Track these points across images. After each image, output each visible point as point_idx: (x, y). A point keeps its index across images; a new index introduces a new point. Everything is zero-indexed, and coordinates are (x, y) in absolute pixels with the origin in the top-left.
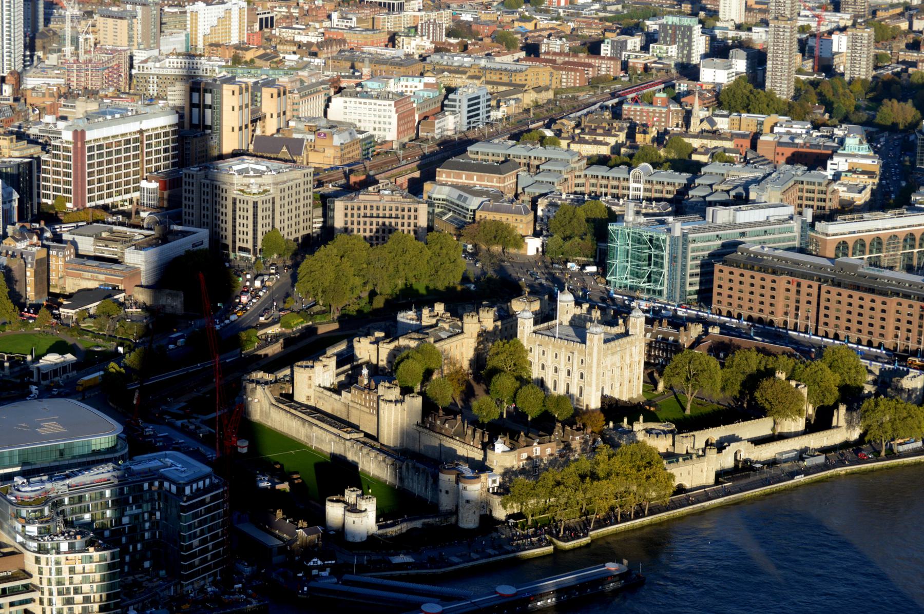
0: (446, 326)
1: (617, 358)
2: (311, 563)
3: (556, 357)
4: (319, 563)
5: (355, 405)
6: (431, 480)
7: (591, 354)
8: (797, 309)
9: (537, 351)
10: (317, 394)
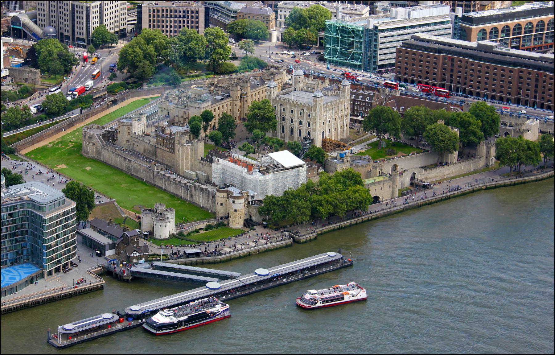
0: (220, 93)
2: (132, 255)
3: (292, 112)
4: (137, 254)
5: (160, 147)
6: (211, 197)
7: (315, 111)
8: (452, 76)
9: (279, 108)
10: (134, 139)
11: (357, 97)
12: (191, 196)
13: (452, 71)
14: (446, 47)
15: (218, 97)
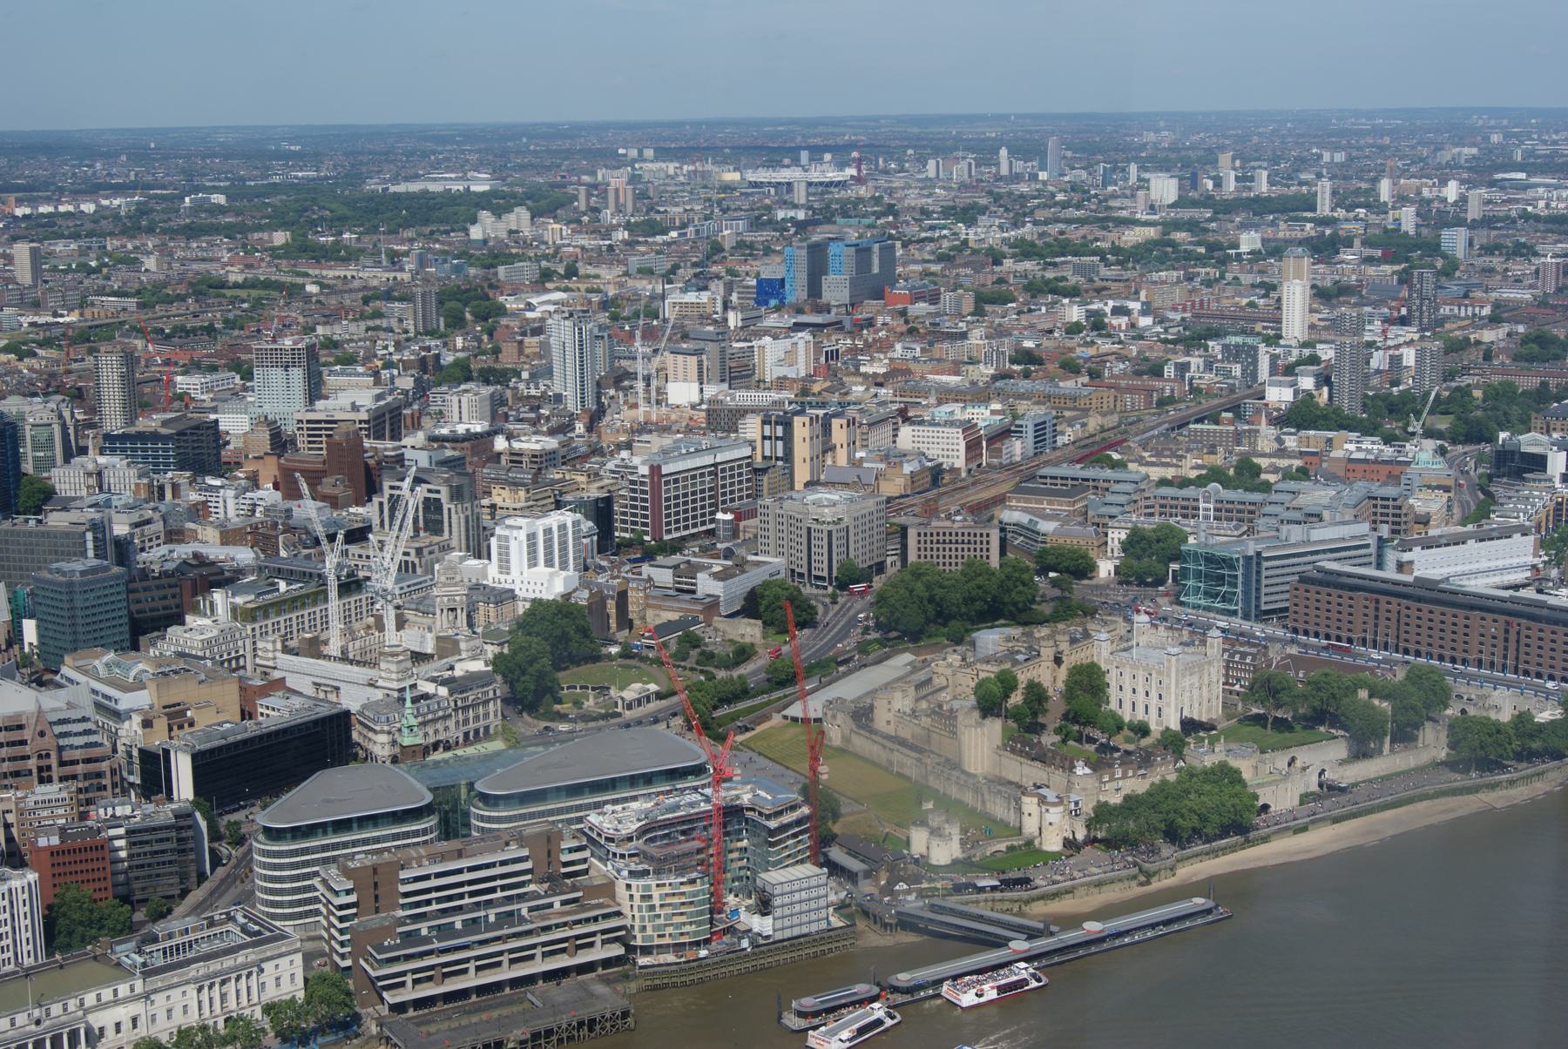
1: (1195, 679)
7: (1169, 676)
8: (1376, 625)
11: (1232, 656)
12: (984, 803)
13: (1377, 617)
14: (1366, 583)
15: (1020, 657)
